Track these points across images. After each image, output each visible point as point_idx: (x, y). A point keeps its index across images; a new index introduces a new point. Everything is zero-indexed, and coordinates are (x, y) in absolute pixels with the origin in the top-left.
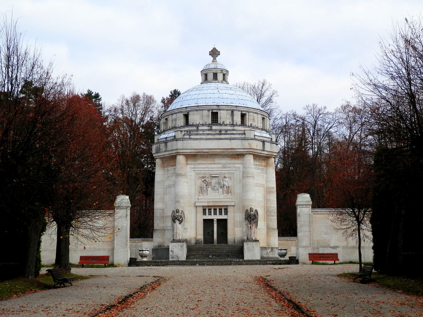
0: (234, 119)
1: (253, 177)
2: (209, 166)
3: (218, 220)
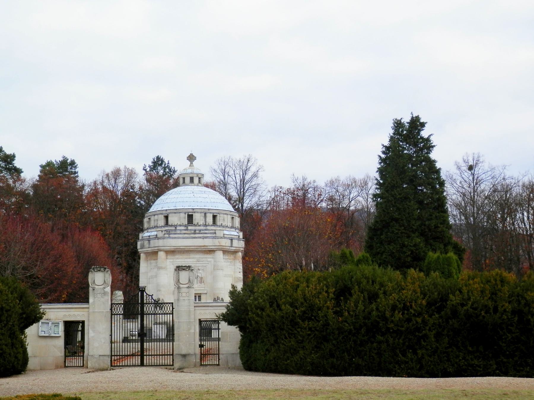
1: (222, 269)
2: (186, 260)
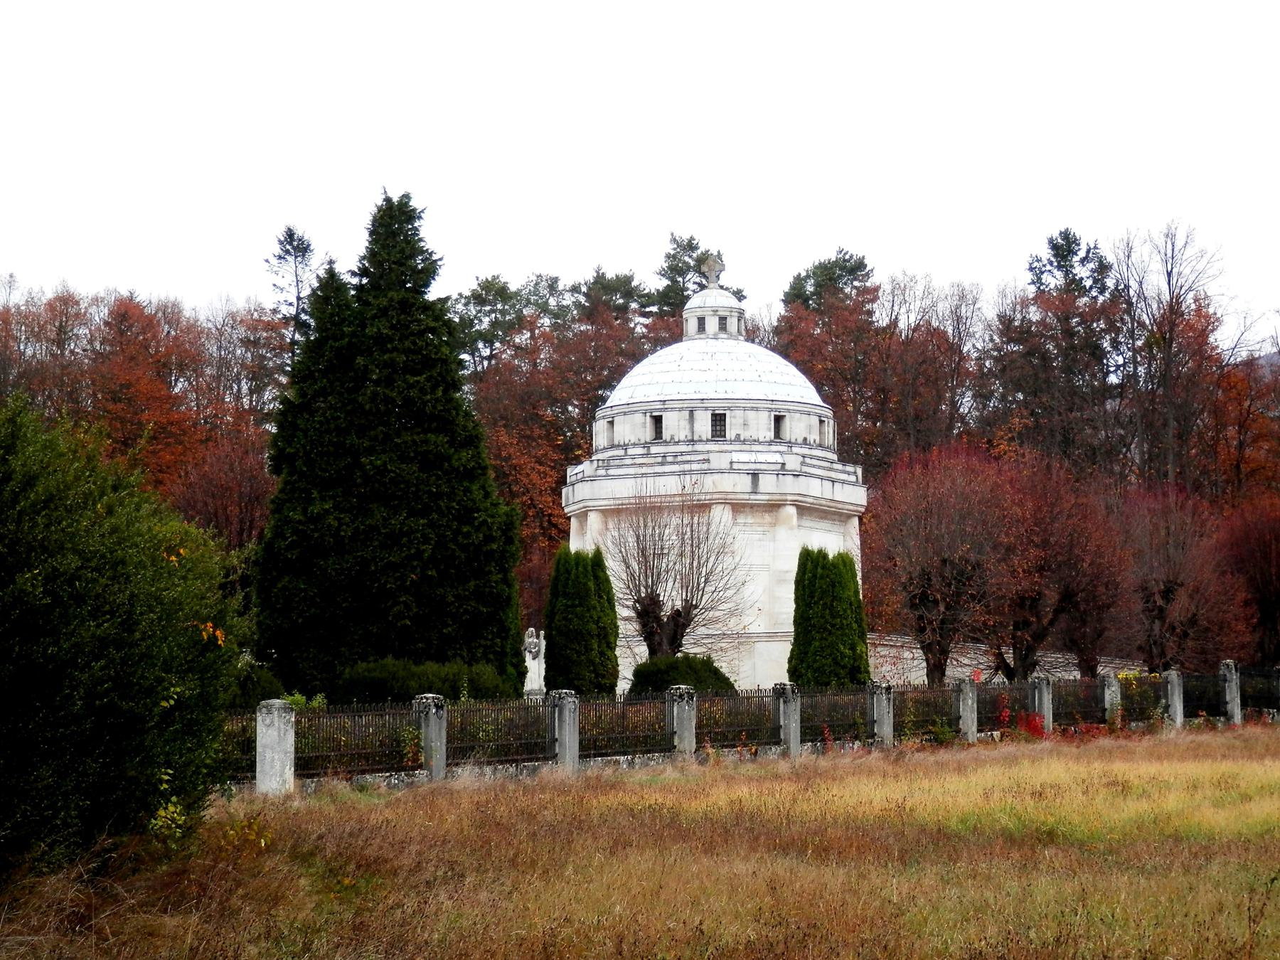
0: (695, 429)
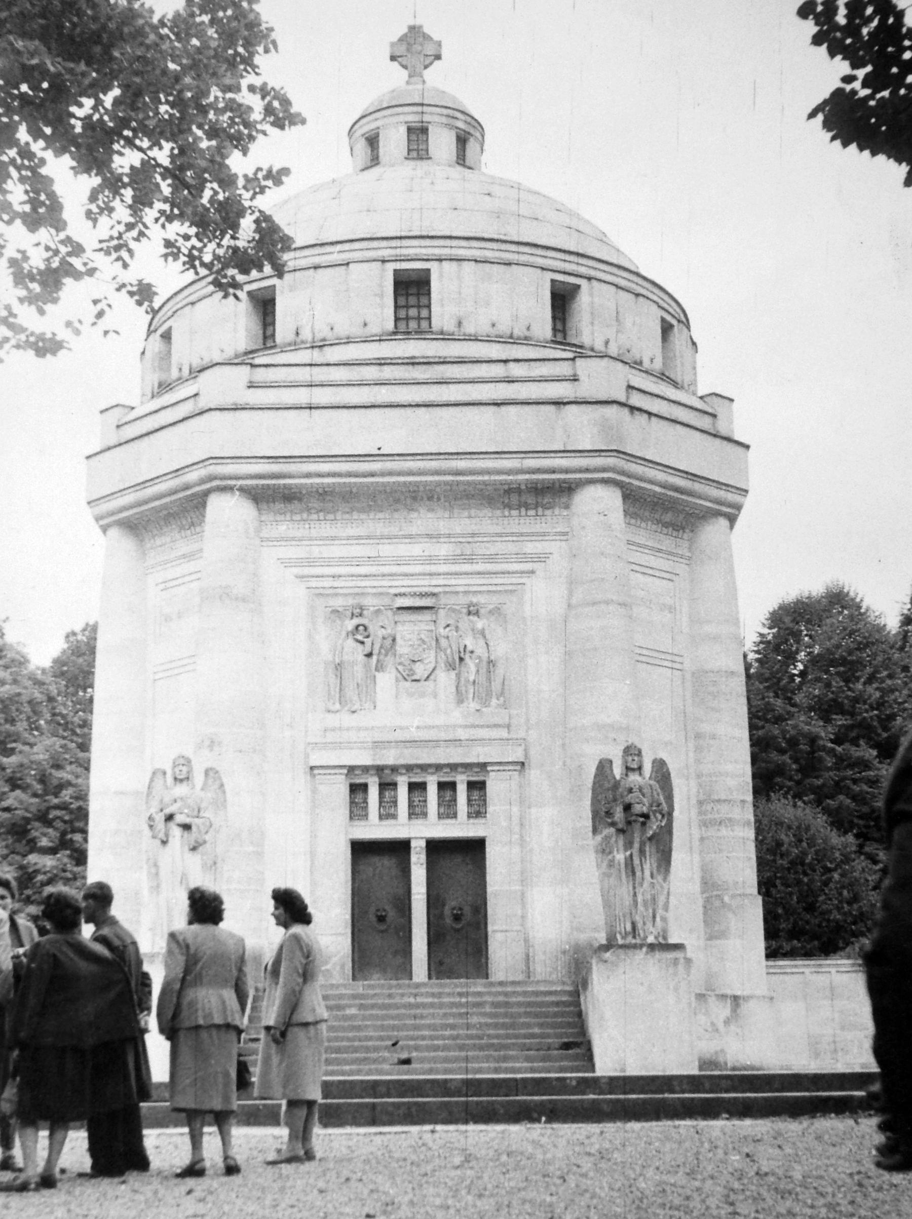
2: (386, 550)
3: (435, 847)
